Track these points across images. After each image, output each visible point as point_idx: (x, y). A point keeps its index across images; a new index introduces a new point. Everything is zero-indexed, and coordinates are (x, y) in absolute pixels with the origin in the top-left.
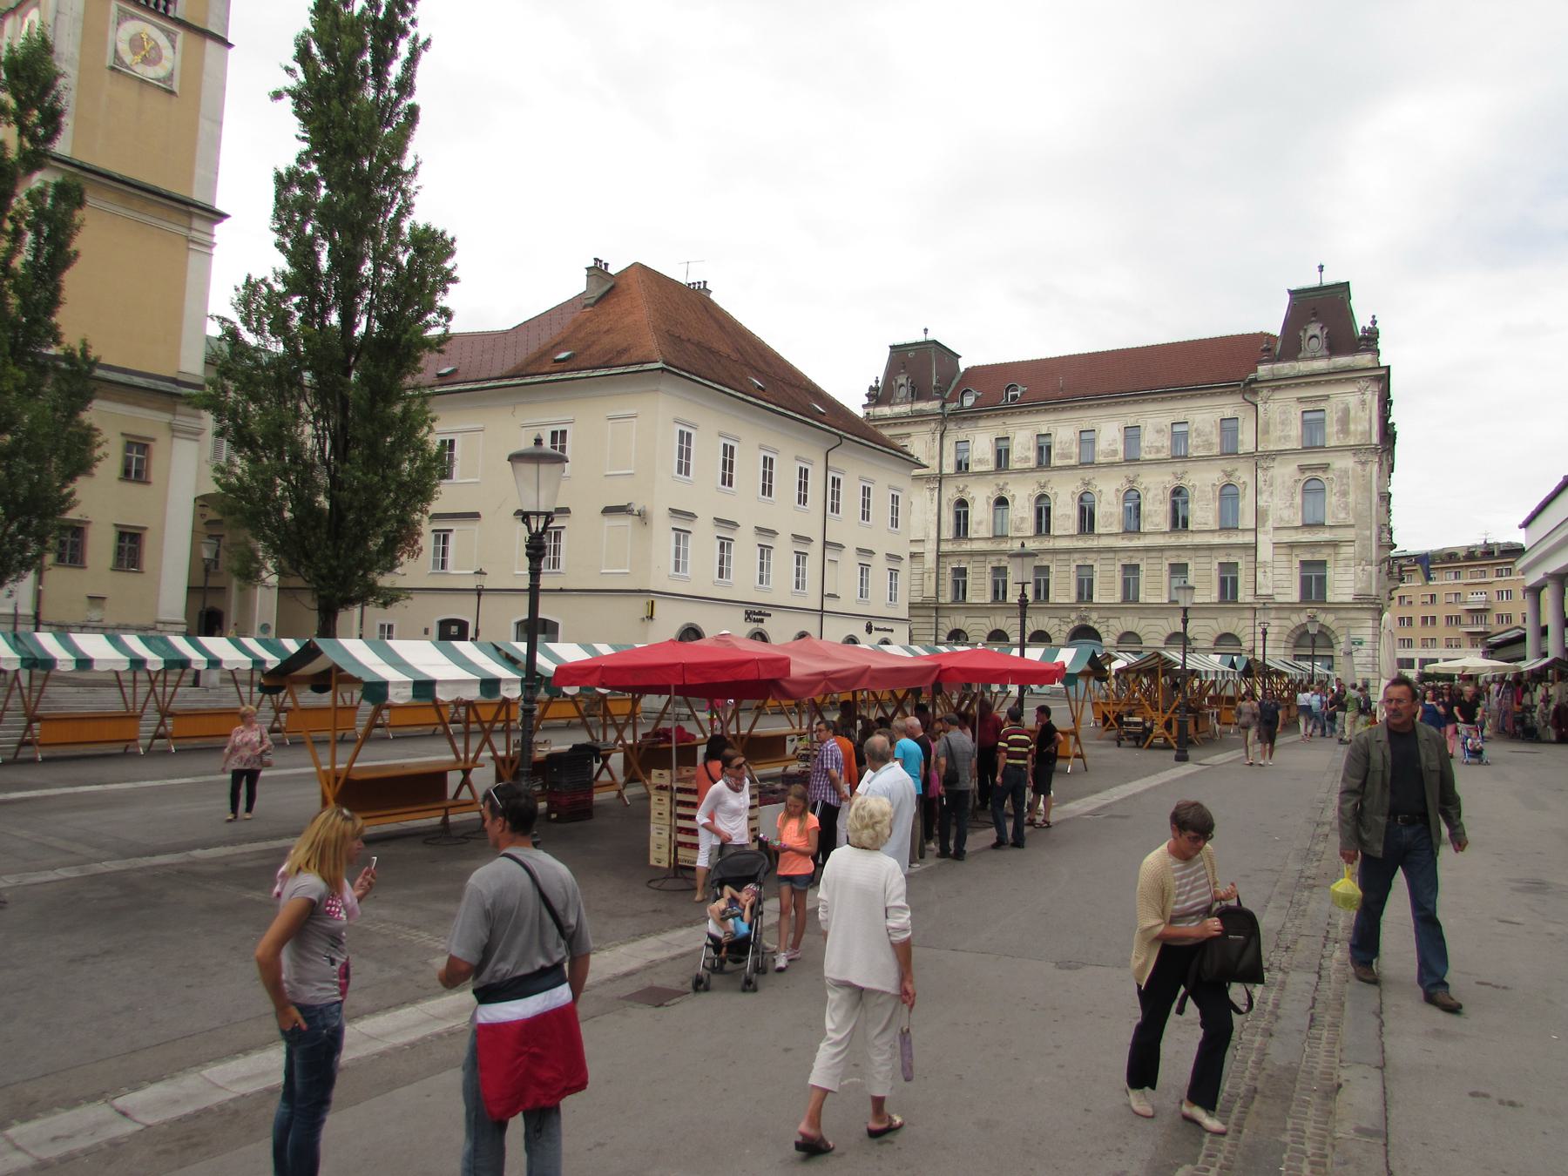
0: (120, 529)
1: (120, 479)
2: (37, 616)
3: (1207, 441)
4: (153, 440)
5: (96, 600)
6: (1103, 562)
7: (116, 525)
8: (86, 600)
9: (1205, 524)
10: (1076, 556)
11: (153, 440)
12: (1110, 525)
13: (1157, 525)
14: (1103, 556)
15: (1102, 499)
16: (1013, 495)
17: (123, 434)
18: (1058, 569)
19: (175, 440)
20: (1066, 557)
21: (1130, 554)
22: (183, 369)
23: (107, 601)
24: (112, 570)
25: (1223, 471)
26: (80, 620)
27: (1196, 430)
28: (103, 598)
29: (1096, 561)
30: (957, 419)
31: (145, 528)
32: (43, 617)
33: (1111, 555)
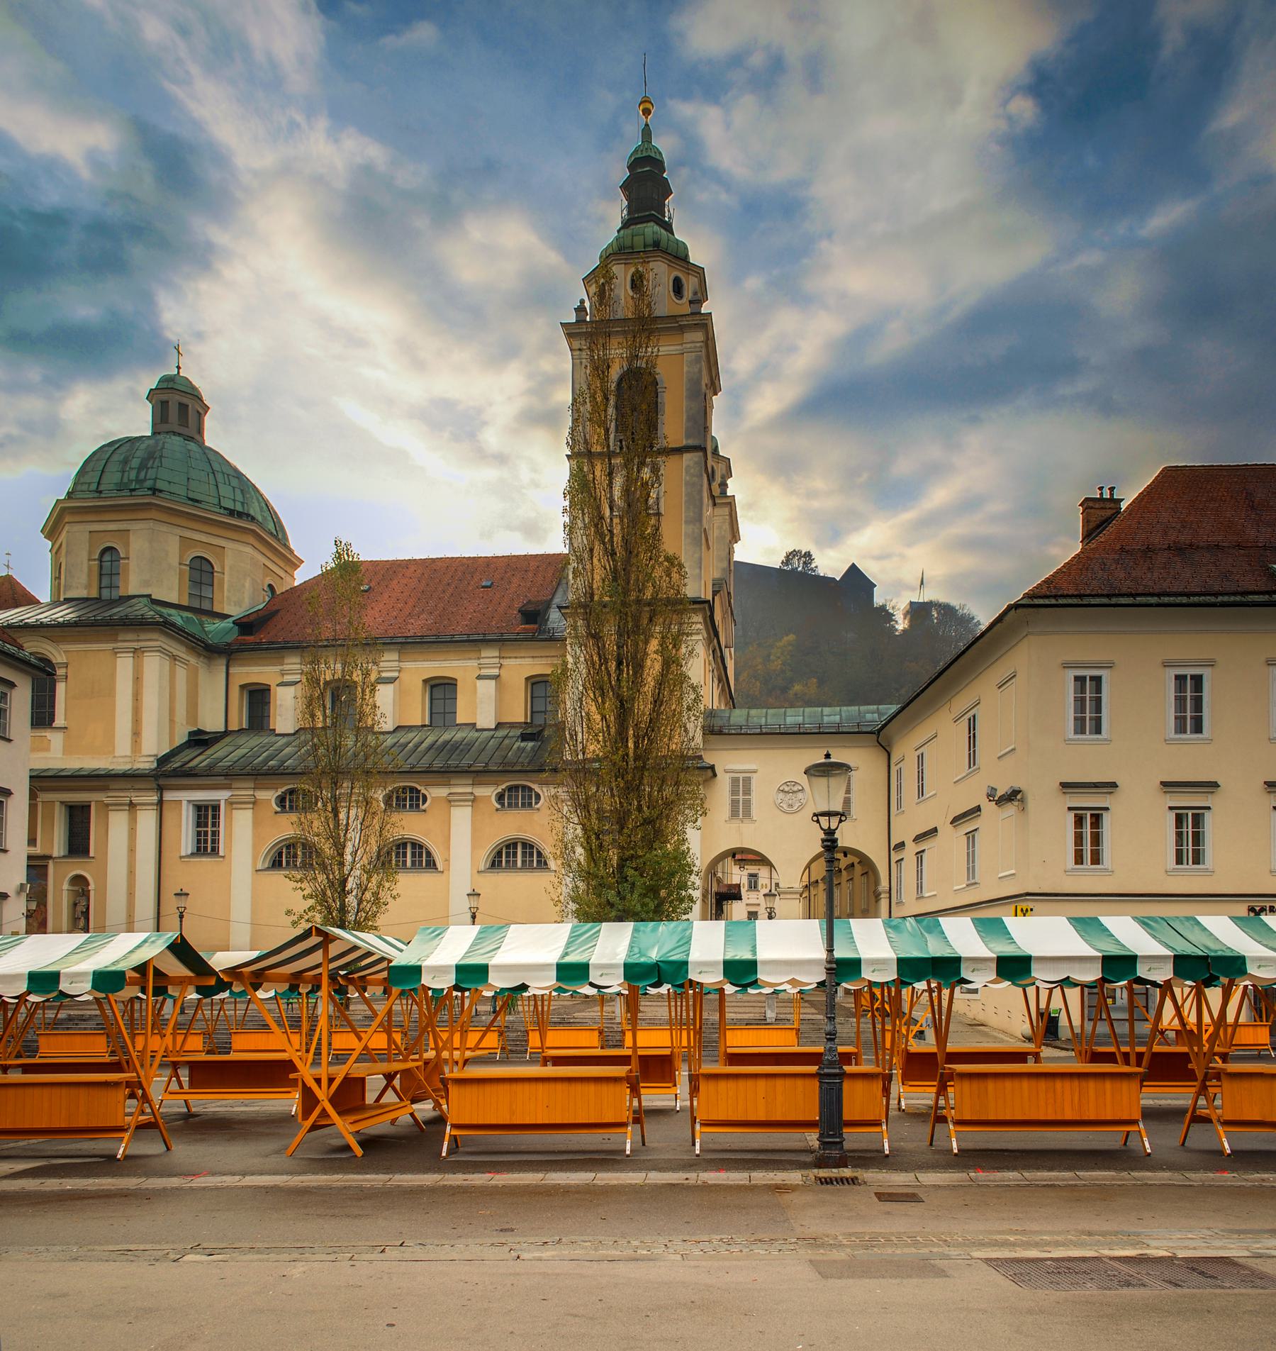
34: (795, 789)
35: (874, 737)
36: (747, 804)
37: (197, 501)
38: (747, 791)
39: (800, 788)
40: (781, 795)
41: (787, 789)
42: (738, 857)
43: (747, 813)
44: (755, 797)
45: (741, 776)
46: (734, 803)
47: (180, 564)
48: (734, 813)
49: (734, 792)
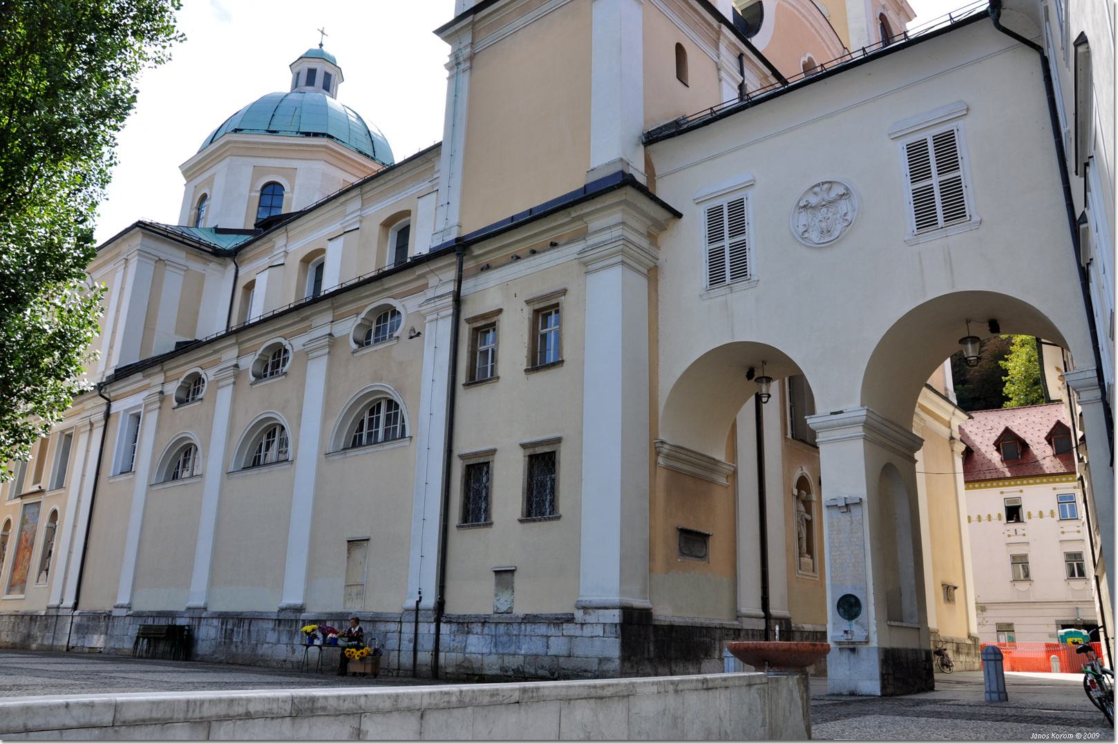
0: (531, 451)
1: (527, 371)
2: (441, 605)
4: (564, 292)
5: (504, 575)
7: (524, 446)
8: (494, 574)
11: (564, 292)
17: (528, 302)
19: (589, 277)
22: (592, 167)
23: (516, 574)
24: (521, 521)
26: (486, 609)
28: (512, 572)
31: (558, 440)
32: (451, 609)
34: (833, 195)
35: (988, 23)
36: (740, 251)
37: (275, 132)
38: (738, 227)
39: (842, 191)
40: (804, 218)
41: (814, 200)
42: (757, 374)
43: (740, 270)
44: (752, 236)
45: (724, 202)
46: (716, 258)
47: (251, 191)
48: (716, 277)
49: (715, 234)
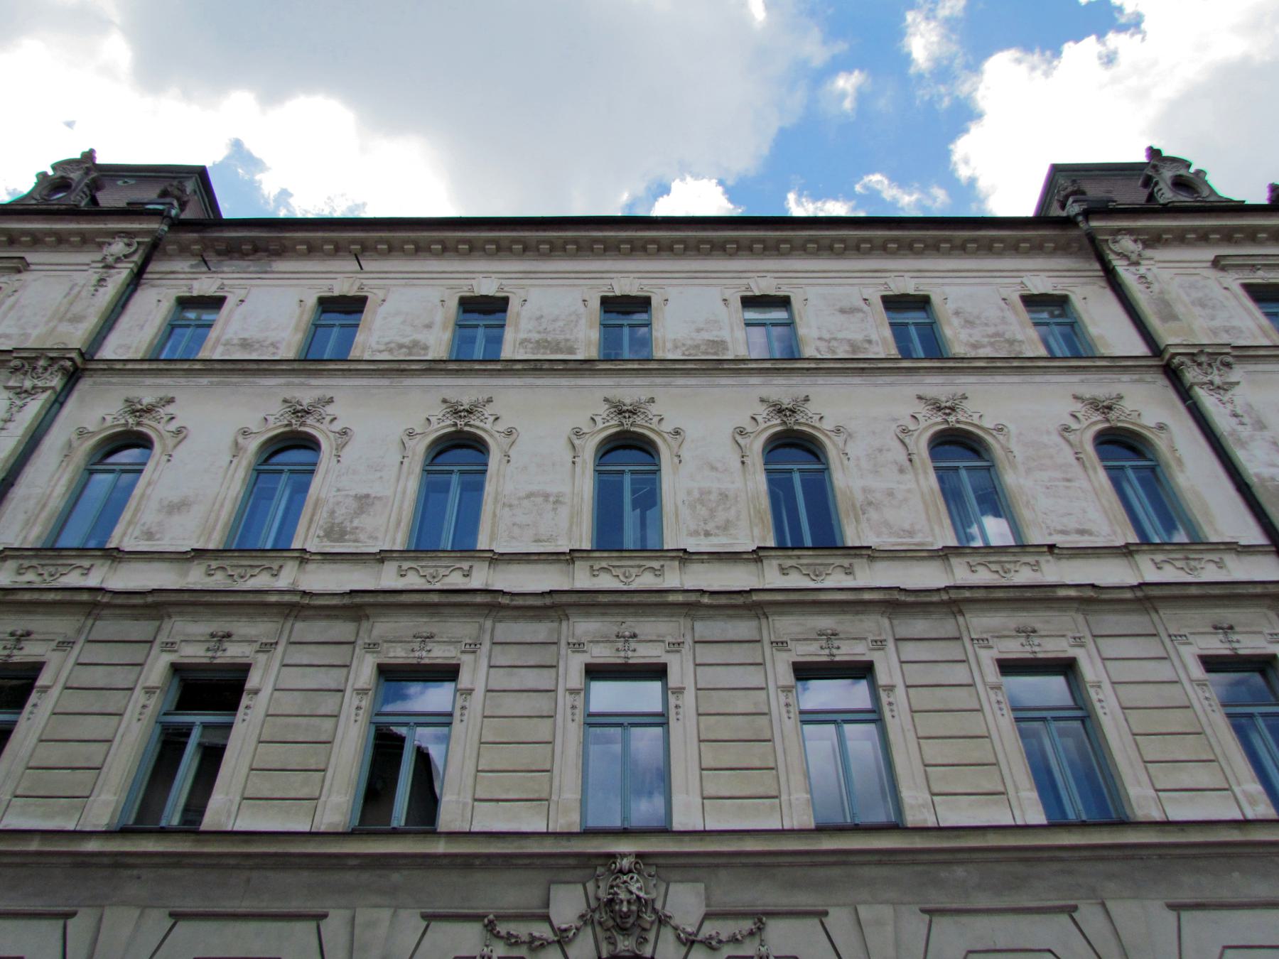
3: (997, 335)
6: (706, 654)
9: (1082, 532)
10: (584, 627)
12: (726, 527)
13: (911, 533)
14: (706, 628)
15: (685, 454)
16: (344, 433)
18: (501, 680)
20: (539, 630)
21: (826, 622)
25: (1076, 397)
27: (957, 313)
29: (676, 646)
30: (208, 246)
33: (743, 628)
